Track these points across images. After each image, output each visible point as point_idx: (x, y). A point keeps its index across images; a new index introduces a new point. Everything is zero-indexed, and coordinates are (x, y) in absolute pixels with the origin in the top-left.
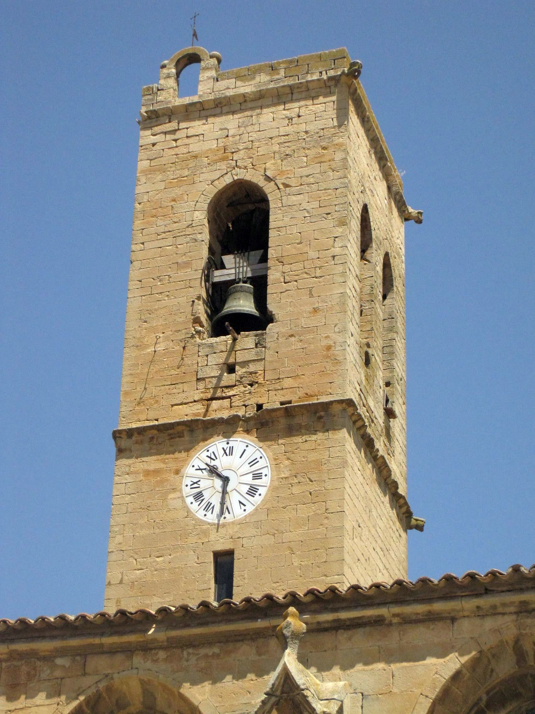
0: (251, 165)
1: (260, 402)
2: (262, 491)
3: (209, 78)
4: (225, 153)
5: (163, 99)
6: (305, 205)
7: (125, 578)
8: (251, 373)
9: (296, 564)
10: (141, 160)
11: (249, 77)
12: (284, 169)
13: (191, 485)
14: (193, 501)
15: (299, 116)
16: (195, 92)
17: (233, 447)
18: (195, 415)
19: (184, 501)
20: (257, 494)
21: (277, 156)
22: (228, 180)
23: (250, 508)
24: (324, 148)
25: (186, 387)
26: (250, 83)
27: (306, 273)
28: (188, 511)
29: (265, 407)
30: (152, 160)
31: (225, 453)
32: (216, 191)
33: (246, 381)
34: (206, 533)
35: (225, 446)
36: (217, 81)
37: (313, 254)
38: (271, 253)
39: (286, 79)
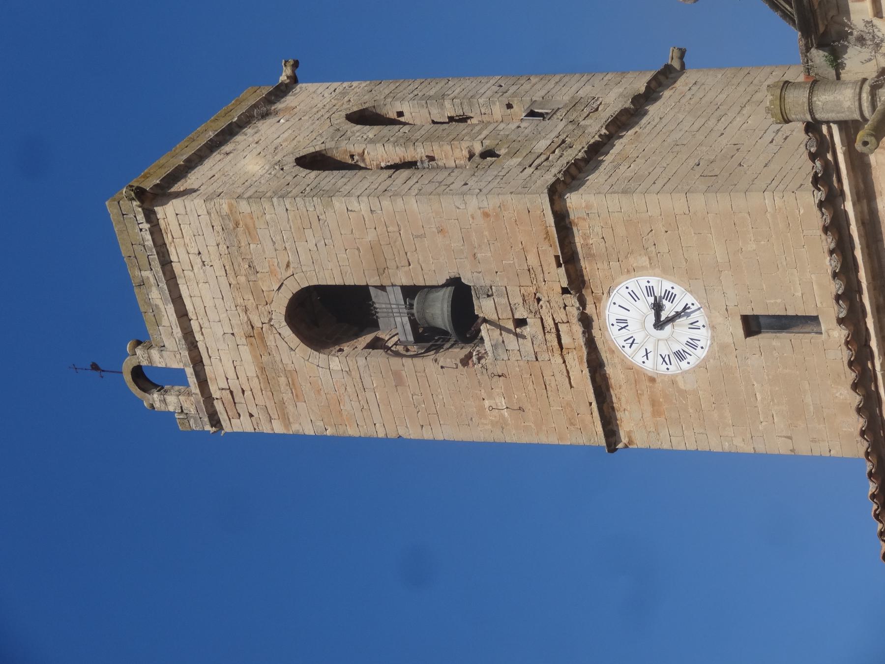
0: (266, 307)
1: (560, 291)
2: (667, 285)
3: (162, 356)
4: (254, 336)
5: (194, 407)
7: (784, 434)
8: (524, 300)
9: (754, 247)
10: (273, 430)
11: (156, 311)
12: (268, 269)
13: (667, 364)
14: (685, 361)
15: (199, 253)
16: (182, 371)
17: (617, 320)
18: (581, 363)
19: (686, 372)
20: (672, 291)
21: (252, 278)
22: (287, 332)
24: (237, 225)
26: (163, 310)
27: (395, 242)
28: (699, 366)
29: (565, 285)
30: (270, 417)
31: (624, 327)
33: (534, 306)
34: (723, 348)
35: (616, 327)
36: (164, 346)
38: (373, 281)
39: (153, 269)
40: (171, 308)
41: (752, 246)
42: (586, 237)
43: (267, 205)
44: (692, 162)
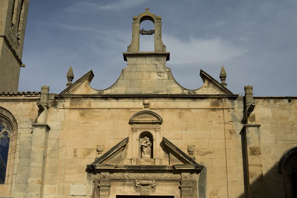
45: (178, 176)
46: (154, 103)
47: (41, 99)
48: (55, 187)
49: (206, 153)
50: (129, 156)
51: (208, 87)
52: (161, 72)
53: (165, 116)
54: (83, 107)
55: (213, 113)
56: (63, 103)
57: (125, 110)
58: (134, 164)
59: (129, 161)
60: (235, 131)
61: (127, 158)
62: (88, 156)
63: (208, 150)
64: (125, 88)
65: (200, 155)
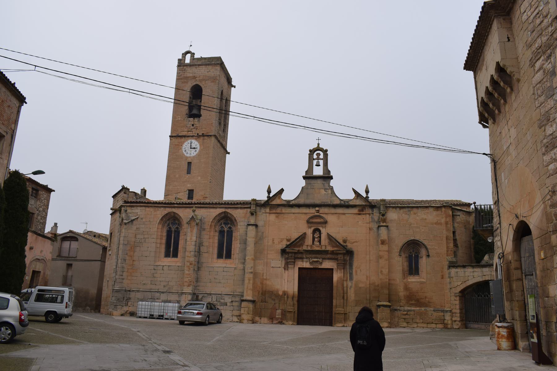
2: (198, 151)
6: (210, 92)
18: (185, 134)
22: (195, 84)
23: (195, 154)
24: (214, 79)
25: (184, 128)
29: (199, 134)
32: (192, 86)
37: (210, 103)
40: (201, 63)
41: (203, 166)
42: (207, 139)
43: (217, 86)
44: (216, 157)
45: (336, 257)
46: (323, 210)
47: (252, 207)
48: (262, 262)
49: (354, 242)
50: (306, 244)
51: (357, 199)
52: (327, 189)
53: (329, 218)
54: (278, 212)
55: (360, 216)
56: (265, 209)
57: (303, 214)
58: (309, 248)
59: (306, 246)
60: (373, 228)
61: (305, 245)
62: (281, 243)
63: (356, 240)
64: (304, 200)
65: (350, 243)
